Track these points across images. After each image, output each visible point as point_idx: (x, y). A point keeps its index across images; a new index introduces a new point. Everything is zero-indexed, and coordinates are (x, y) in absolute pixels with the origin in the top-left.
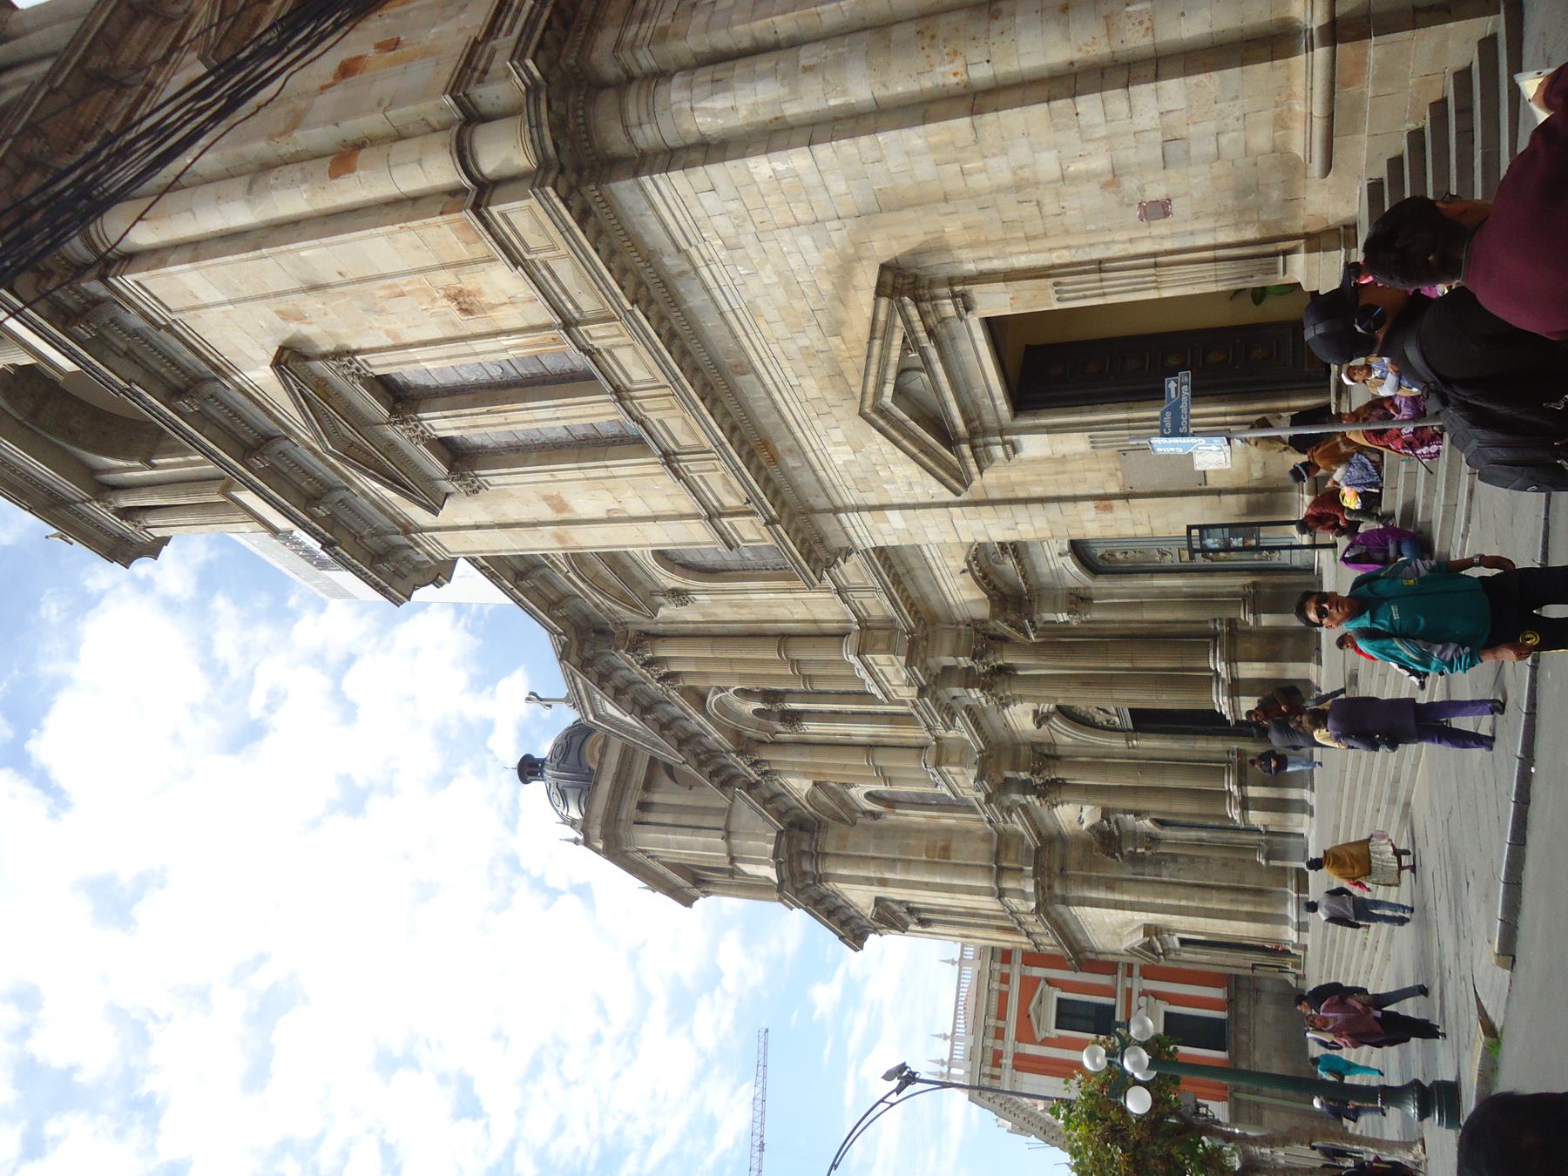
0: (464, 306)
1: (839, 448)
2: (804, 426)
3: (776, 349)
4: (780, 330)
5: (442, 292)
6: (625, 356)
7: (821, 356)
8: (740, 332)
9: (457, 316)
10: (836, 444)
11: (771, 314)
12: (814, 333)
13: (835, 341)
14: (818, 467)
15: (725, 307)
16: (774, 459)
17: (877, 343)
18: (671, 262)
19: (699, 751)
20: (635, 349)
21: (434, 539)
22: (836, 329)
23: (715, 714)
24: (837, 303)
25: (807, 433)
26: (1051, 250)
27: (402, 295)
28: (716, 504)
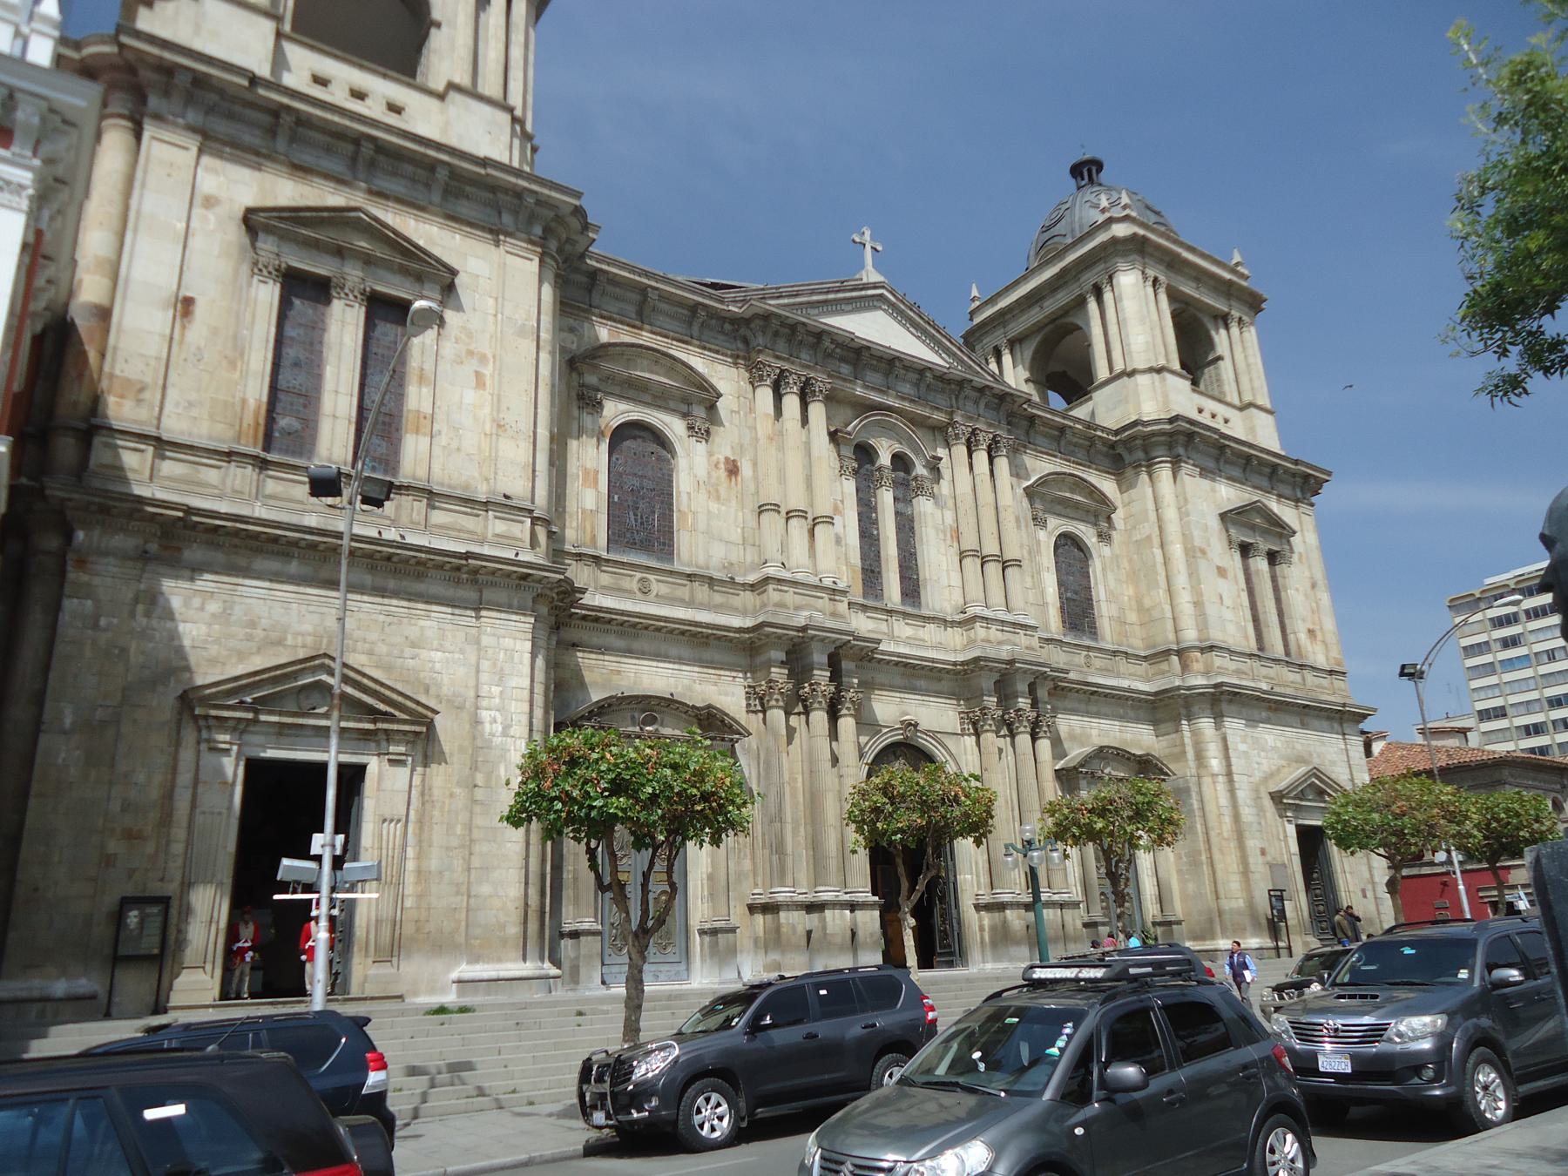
6: (1297, 677)
19: (838, 350)
23: (891, 416)
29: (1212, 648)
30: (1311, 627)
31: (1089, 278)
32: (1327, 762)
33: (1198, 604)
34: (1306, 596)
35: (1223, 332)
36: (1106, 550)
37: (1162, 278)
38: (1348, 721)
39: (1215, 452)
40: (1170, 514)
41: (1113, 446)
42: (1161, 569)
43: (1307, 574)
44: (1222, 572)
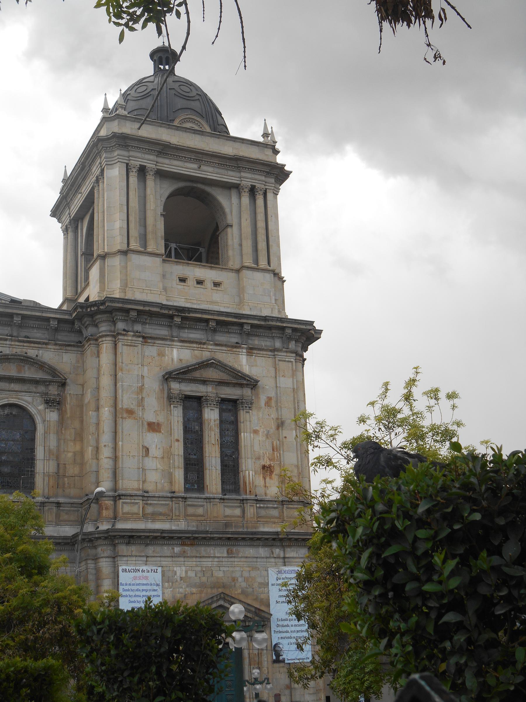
0: (266, 469)
1: (184, 572)
2: (199, 563)
3: (237, 569)
4: (246, 574)
5: (272, 465)
7: (233, 584)
8: (247, 560)
9: (263, 463)
10: (186, 572)
11: (253, 574)
12: (244, 585)
13: (240, 591)
14: (174, 559)
15: (259, 560)
16: (183, 544)
17: (253, 610)
18: (277, 551)
20: (239, 517)
21: (135, 346)
22: (243, 592)
24: (255, 597)
25: (195, 563)
26: (268, 668)
27: (273, 450)
28: (149, 502)
29: (120, 496)
30: (267, 463)
31: (95, 170)
32: (256, 585)
33: (115, 459)
34: (267, 436)
35: (235, 200)
36: (53, 416)
37: (150, 165)
38: (289, 546)
39: (165, 321)
40: (106, 381)
41: (71, 322)
42: (92, 429)
43: (274, 415)
44: (153, 427)
